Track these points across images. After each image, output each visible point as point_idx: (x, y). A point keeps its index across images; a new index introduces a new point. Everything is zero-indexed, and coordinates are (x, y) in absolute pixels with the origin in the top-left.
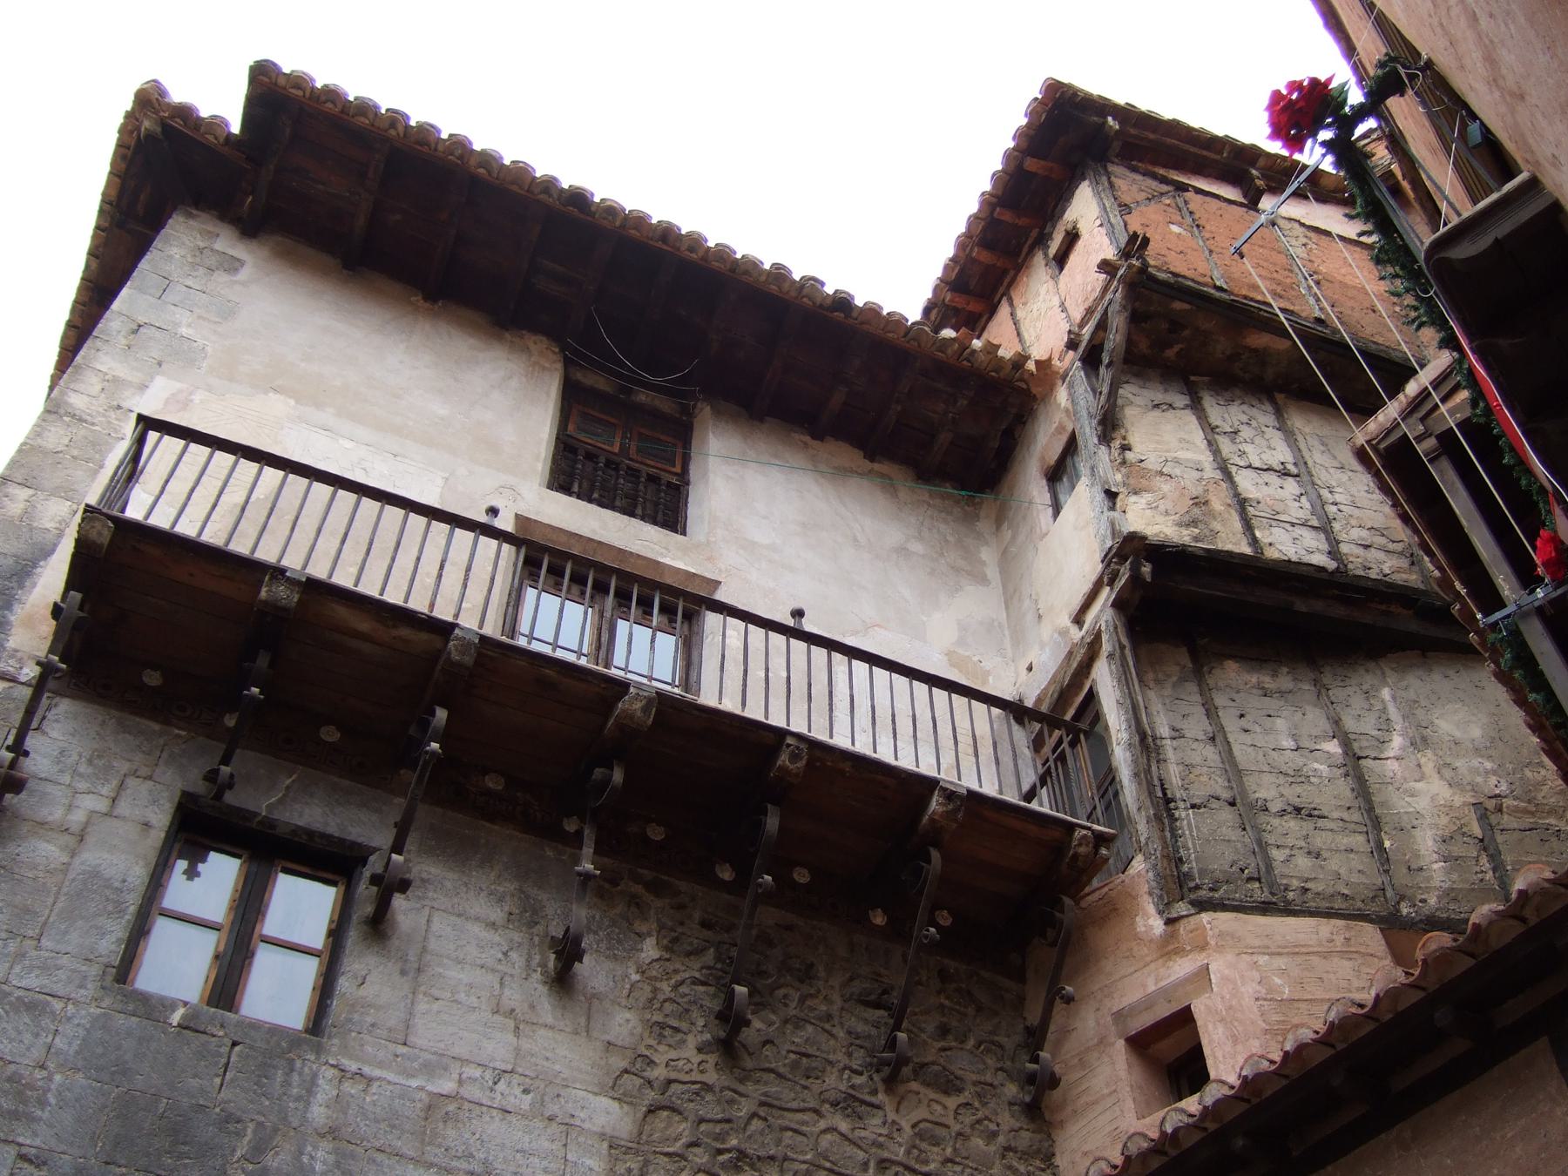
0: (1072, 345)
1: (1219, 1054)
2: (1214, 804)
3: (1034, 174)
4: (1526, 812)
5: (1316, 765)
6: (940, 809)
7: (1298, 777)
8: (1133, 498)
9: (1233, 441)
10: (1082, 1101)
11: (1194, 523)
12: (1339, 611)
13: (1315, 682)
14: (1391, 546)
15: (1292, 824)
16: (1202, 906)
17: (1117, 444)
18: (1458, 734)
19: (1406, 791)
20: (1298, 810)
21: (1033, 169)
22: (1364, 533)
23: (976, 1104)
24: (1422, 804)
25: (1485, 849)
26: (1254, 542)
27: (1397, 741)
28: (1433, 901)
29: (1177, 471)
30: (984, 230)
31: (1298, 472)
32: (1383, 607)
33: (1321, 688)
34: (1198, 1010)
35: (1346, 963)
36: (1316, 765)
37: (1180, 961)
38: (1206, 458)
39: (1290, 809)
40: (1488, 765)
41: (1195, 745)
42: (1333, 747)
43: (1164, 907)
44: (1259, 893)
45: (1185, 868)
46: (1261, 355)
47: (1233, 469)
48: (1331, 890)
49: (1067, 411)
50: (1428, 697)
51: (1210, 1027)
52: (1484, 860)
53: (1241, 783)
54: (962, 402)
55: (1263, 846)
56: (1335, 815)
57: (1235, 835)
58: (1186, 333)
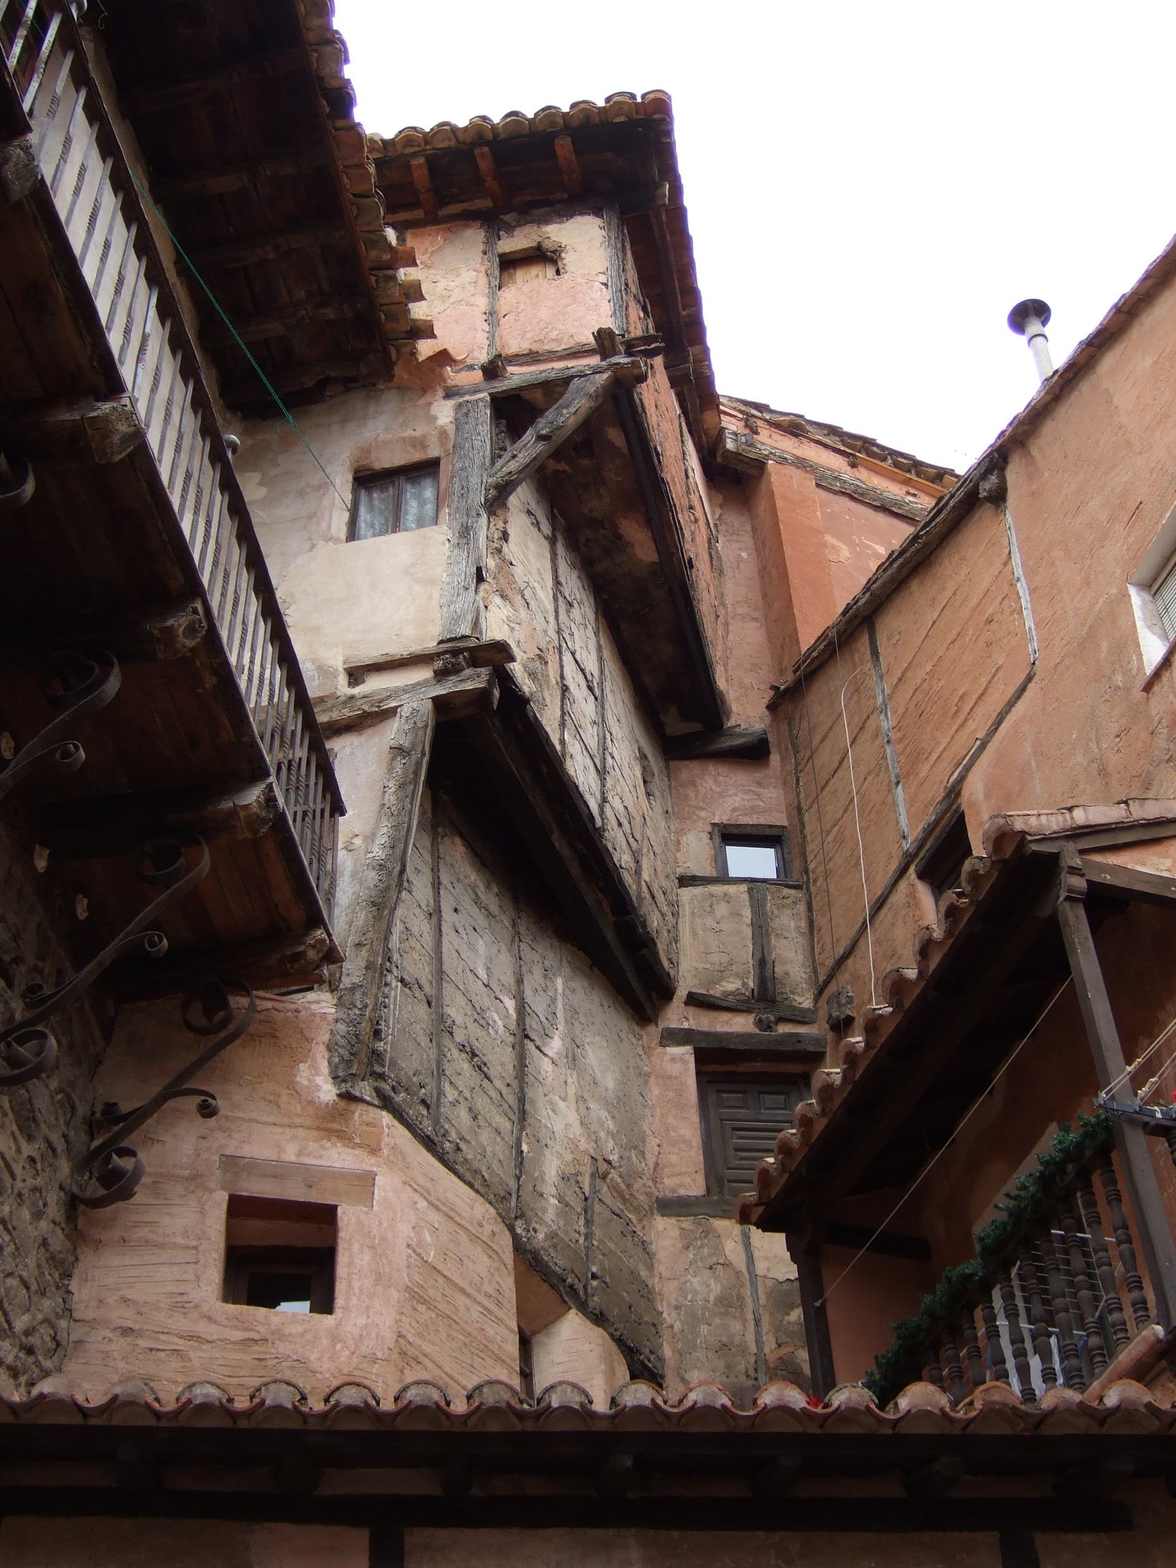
0: (492, 371)
1: (356, 1284)
2: (418, 993)
3: (554, 155)
4: (621, 1195)
5: (496, 1017)
6: (255, 809)
7: (480, 1018)
8: (498, 600)
10: (143, 1233)
11: (532, 675)
14: (631, 840)
16: (386, 1103)
18: (598, 1075)
20: (474, 1055)
21: (560, 152)
22: (622, 809)
23: (39, 1166)
24: (558, 1125)
25: (586, 1212)
26: (562, 742)
27: (555, 1045)
28: (541, 1236)
29: (533, 604)
30: (447, 151)
32: (601, 896)
33: (517, 937)
34: (348, 1216)
35: (486, 1259)
36: (496, 1017)
37: (340, 1147)
39: (468, 1049)
40: (611, 1125)
41: (417, 911)
42: (510, 1004)
44: (428, 1127)
45: (380, 1046)
47: (564, 645)
48: (475, 1165)
49: (443, 434)
51: (356, 1247)
52: (582, 1222)
53: (440, 988)
54: (330, 313)
55: (440, 1073)
57: (424, 1041)
58: (585, 462)
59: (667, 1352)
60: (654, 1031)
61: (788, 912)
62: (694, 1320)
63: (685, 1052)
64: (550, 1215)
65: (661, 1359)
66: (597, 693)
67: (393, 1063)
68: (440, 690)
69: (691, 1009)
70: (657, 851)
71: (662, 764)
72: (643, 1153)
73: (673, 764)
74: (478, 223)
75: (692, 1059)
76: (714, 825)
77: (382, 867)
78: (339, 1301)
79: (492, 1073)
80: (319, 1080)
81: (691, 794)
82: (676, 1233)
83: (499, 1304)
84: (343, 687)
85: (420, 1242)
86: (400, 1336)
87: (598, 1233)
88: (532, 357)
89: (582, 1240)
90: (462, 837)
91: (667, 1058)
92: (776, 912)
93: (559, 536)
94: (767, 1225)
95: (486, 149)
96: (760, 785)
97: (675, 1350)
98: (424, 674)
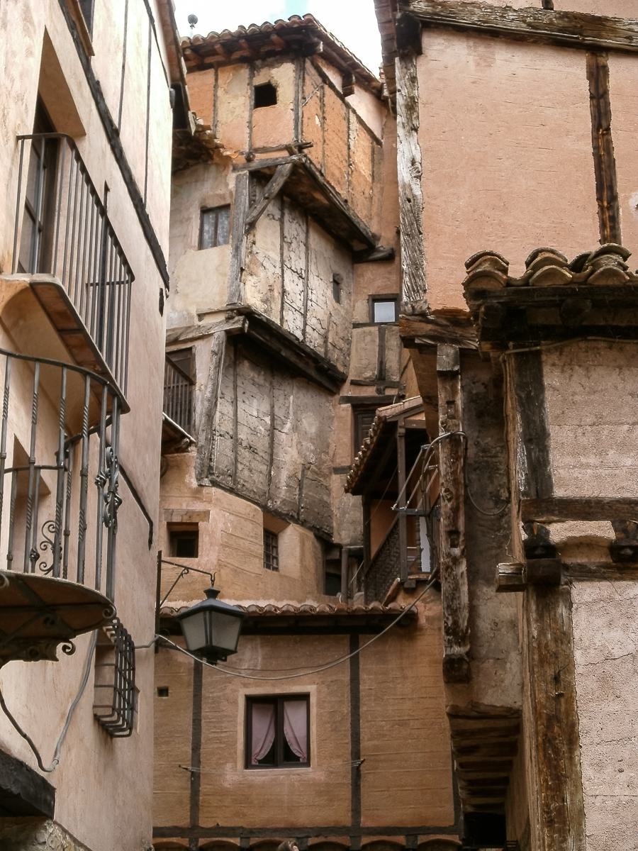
2: (227, 436)
5: (261, 428)
8: (250, 278)
9: (289, 247)
12: (293, 359)
13: (271, 383)
15: (247, 454)
16: (215, 484)
17: (251, 237)
19: (285, 450)
20: (251, 447)
24: (287, 458)
25: (299, 485)
26: (282, 319)
27: (288, 425)
30: (228, 40)
31: (303, 277)
34: (202, 525)
35: (251, 525)
36: (261, 428)
38: (278, 258)
40: (312, 448)
42: (268, 420)
43: (199, 479)
44: (231, 484)
46: (314, 200)
49: (231, 193)
50: (303, 406)
51: (204, 536)
52: (298, 489)
56: (261, 454)
59: (335, 524)
60: (337, 397)
61: (394, 337)
62: (344, 513)
63: (347, 406)
64: (283, 493)
65: (332, 528)
66: (304, 276)
67: (217, 468)
68: (228, 327)
69: (353, 386)
70: (338, 323)
71: (349, 267)
72: (327, 453)
73: (355, 265)
74: (246, 65)
75: (350, 409)
76: (369, 295)
77: (209, 400)
78: (199, 554)
79: (258, 452)
80: (192, 480)
81: (362, 281)
82: (339, 481)
83: (256, 538)
84: (196, 322)
85: (226, 528)
86: (219, 560)
87: (304, 491)
88: (264, 150)
89: (297, 497)
90: (246, 358)
91: (341, 409)
92: (389, 338)
93: (286, 212)
94: (354, 493)
95: (243, 41)
96: (390, 273)
97: (337, 524)
98: (222, 317)
